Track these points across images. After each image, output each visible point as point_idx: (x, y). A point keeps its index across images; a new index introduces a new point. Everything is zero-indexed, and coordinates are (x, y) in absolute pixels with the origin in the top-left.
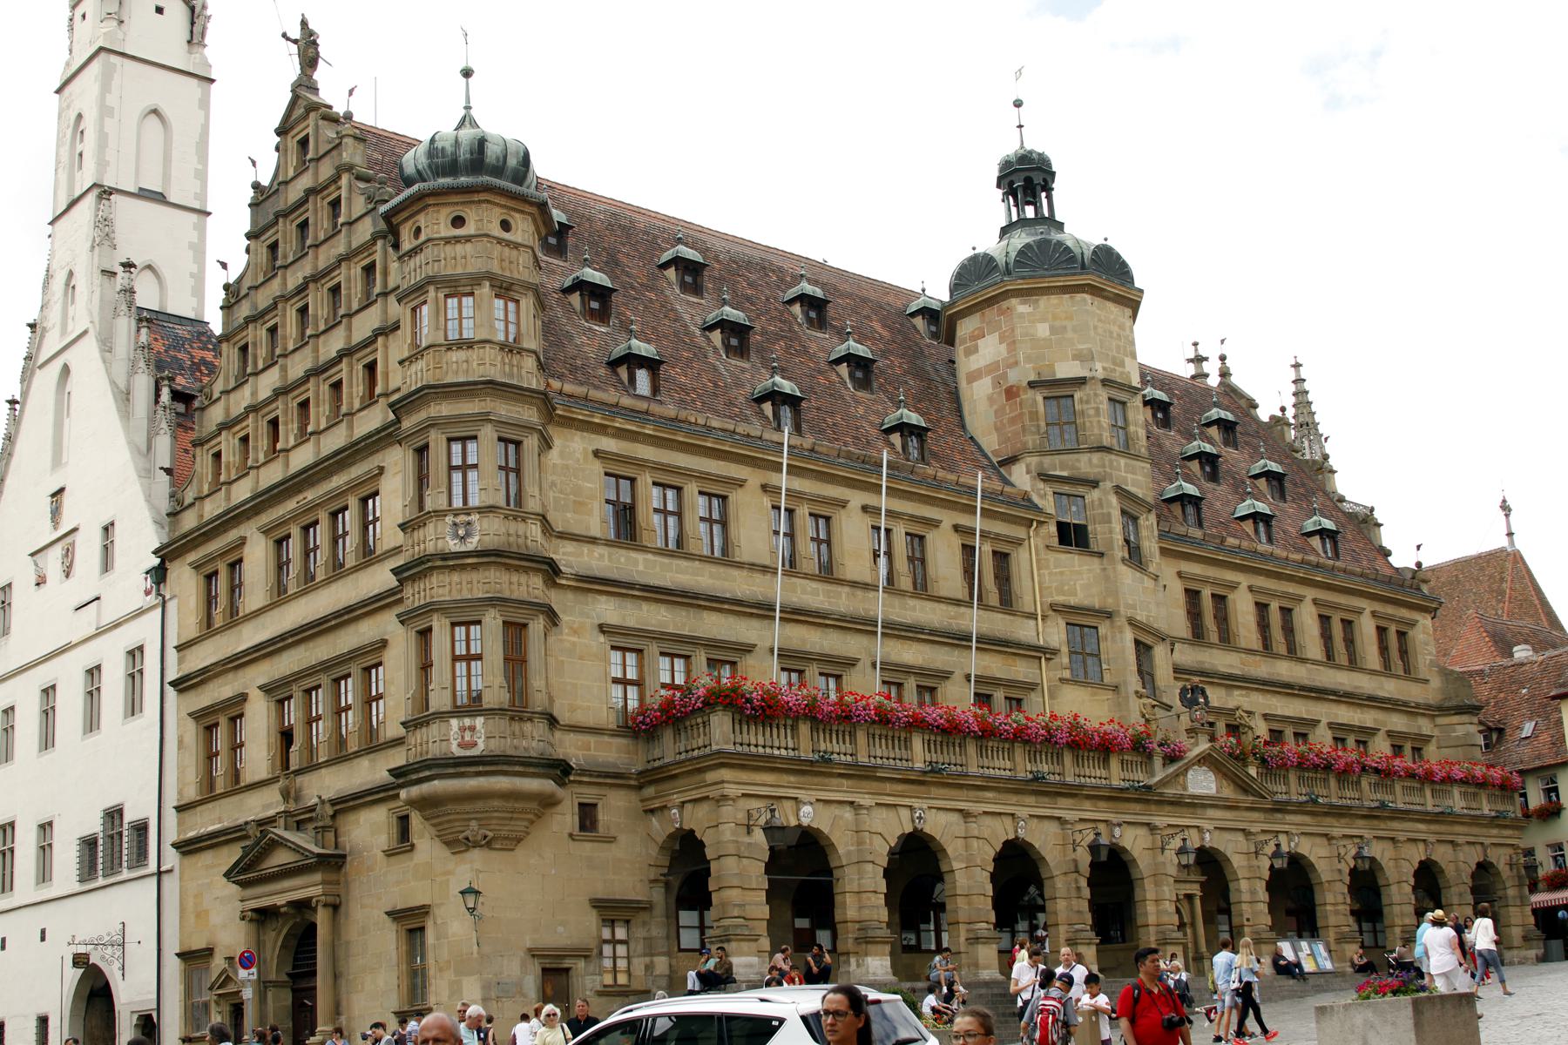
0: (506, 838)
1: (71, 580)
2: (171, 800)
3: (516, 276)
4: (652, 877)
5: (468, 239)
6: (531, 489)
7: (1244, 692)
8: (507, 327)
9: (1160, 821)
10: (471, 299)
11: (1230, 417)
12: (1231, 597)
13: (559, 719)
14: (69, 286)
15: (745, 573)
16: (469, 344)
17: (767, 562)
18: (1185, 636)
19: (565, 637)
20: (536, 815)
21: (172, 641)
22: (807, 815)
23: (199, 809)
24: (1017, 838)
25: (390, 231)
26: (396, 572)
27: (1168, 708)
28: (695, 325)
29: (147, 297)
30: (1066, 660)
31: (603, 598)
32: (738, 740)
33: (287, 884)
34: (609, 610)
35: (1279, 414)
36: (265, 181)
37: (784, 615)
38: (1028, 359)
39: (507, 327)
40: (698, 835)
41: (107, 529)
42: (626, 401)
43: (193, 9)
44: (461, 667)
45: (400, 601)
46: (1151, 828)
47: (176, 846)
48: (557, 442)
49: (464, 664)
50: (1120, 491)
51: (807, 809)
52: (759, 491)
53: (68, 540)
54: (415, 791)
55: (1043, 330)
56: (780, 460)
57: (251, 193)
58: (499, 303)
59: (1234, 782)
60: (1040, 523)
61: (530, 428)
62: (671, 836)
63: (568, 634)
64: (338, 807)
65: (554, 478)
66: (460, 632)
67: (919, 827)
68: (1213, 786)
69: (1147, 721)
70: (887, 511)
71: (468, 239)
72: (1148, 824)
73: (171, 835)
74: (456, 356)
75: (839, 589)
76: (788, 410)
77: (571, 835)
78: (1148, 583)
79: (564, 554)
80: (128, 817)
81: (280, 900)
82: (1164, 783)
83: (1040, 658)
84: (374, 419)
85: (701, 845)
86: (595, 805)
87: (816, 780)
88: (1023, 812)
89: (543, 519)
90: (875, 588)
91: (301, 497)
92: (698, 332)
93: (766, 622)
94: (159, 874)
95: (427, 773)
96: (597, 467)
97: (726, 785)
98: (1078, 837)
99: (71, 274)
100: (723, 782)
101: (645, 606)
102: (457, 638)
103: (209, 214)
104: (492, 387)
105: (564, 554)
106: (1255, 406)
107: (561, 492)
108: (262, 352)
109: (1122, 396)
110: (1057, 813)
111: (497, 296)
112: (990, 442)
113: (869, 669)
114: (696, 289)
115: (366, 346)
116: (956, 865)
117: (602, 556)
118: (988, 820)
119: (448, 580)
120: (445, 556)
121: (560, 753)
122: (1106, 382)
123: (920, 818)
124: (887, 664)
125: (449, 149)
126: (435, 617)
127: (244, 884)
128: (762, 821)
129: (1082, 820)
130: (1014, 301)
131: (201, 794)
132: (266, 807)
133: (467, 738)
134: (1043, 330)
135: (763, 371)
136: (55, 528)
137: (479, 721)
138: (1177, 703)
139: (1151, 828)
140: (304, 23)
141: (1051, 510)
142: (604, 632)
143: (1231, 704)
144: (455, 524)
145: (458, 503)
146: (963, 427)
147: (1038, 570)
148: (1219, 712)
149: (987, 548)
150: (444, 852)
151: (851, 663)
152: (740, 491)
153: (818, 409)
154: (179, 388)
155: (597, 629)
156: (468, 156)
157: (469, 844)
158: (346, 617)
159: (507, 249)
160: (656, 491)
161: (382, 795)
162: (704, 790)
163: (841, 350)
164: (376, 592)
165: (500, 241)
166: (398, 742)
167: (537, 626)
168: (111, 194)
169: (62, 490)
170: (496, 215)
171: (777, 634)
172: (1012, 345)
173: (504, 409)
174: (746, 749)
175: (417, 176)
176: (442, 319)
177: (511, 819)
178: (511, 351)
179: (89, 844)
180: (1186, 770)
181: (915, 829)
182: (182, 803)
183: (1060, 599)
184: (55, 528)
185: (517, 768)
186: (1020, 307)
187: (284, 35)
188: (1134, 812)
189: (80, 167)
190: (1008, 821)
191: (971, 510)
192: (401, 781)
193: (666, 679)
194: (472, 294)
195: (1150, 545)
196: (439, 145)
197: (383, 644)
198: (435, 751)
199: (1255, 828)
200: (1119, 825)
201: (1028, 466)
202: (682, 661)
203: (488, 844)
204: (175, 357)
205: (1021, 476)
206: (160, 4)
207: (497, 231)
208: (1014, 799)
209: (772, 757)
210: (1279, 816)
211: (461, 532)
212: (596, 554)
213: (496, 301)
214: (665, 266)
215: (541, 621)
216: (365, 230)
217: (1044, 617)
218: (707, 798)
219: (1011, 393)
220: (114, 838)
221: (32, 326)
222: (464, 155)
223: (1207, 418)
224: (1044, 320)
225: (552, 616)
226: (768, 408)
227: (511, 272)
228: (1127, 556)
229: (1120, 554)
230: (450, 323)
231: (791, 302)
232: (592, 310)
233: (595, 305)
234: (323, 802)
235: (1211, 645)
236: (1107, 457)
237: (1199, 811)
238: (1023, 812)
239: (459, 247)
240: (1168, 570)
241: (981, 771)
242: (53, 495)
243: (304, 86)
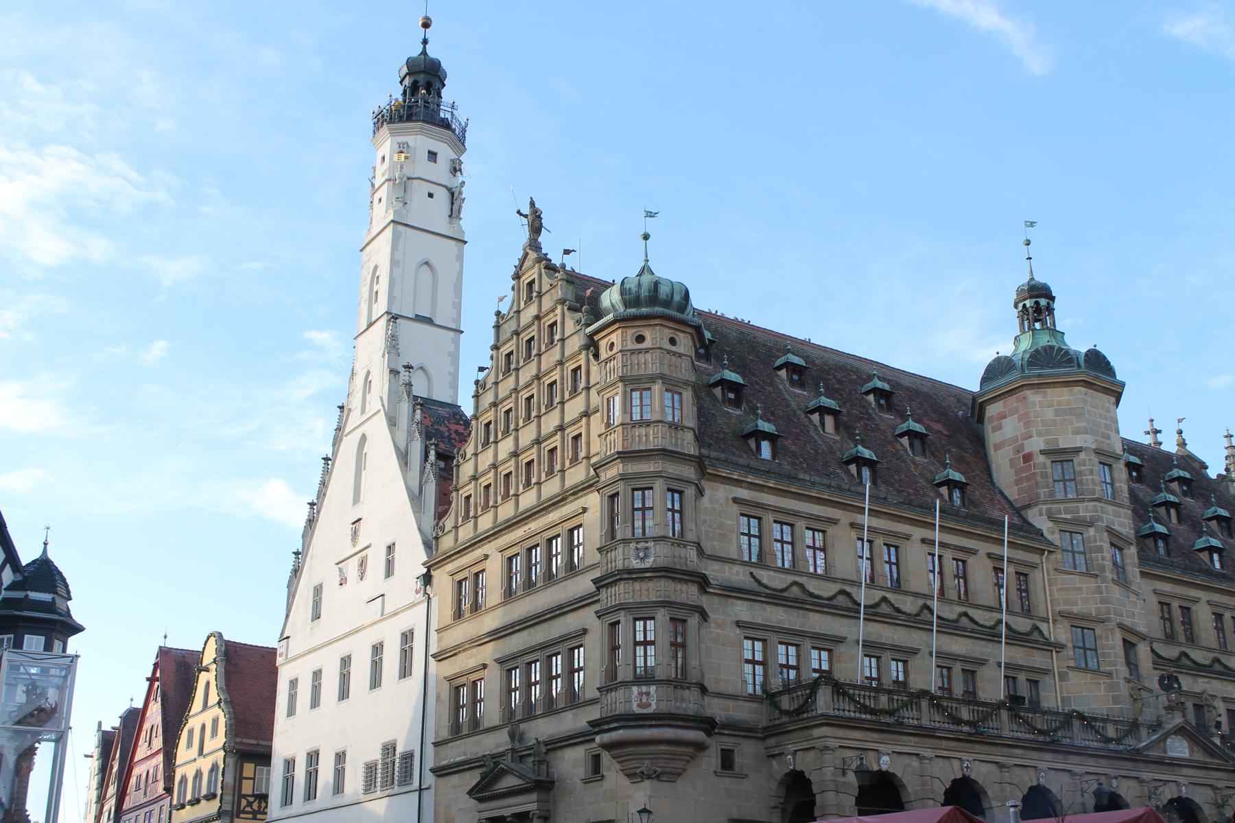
0: (671, 773)
1: (364, 582)
2: (430, 738)
3: (680, 376)
4: (772, 804)
5: (647, 351)
6: (690, 525)
7: (1206, 680)
8: (673, 412)
9: (1146, 776)
10: (649, 392)
11: (1188, 476)
12: (1194, 608)
13: (708, 688)
14: (367, 382)
16: (648, 424)
17: (854, 578)
18: (1160, 637)
19: (713, 630)
20: (691, 757)
21: (434, 626)
22: (885, 763)
23: (450, 745)
24: (1039, 785)
25: (592, 345)
26: (595, 581)
27: (1151, 691)
28: (801, 409)
29: (420, 390)
30: (1071, 653)
31: (739, 602)
32: (836, 706)
33: (512, 801)
34: (742, 610)
35: (1225, 473)
36: (504, 311)
37: (866, 617)
38: (1040, 434)
39: (673, 412)
40: (807, 775)
41: (390, 548)
42: (753, 463)
43: (453, 194)
44: (640, 651)
45: (598, 601)
46: (1140, 781)
47: (433, 770)
48: (707, 492)
49: (642, 648)
50: (1110, 531)
51: (885, 758)
52: (849, 527)
53: (363, 554)
54: (607, 737)
55: (1049, 414)
56: (863, 506)
57: (495, 318)
58: (668, 395)
59: (1202, 748)
60: (1050, 552)
61: (689, 482)
62: (786, 775)
63: (714, 628)
64: (550, 747)
65: (705, 517)
66: (639, 625)
67: (967, 774)
68: (1187, 751)
69: (1135, 700)
70: (939, 542)
72: (1137, 778)
73: (430, 763)
74: (637, 431)
75: (906, 598)
76: (867, 470)
77: (715, 772)
78: (1133, 598)
79: (712, 571)
80: (400, 750)
81: (507, 812)
82: (1147, 747)
83: (1052, 651)
84: (577, 475)
85: (809, 782)
86: (733, 751)
87: (892, 737)
88: (1043, 765)
89: (699, 547)
91: (526, 527)
92: (803, 416)
93: (854, 621)
94: (420, 790)
95: (615, 725)
96: (735, 509)
97: (828, 739)
98: (1085, 786)
99: (368, 372)
100: (826, 737)
101: (768, 608)
102: (638, 629)
104: (665, 453)
105: (712, 571)
106: (1206, 468)
107: (710, 527)
108: (501, 427)
109: (1108, 460)
110: (1068, 767)
111: (667, 390)
112: (1012, 493)
113: (927, 657)
114: (801, 384)
115: (574, 424)
116: (994, 804)
117: (738, 572)
118: (1017, 770)
119: (631, 588)
120: (630, 571)
121: (708, 712)
122: (1098, 452)
123: (967, 767)
124: (941, 653)
125: (634, 289)
126: (623, 613)
127: (481, 800)
128: (854, 766)
129: (1087, 773)
130: (1028, 393)
131: (452, 735)
132: (498, 746)
134: (1049, 414)
135: (849, 441)
136: (354, 546)
137: (653, 689)
138: (1156, 686)
139: (1140, 781)
140: (532, 204)
141: (1058, 543)
142: (739, 627)
143: (1198, 689)
144: (637, 549)
145: (639, 532)
146: (992, 482)
147: (1049, 586)
148: (1189, 694)
149: (1012, 570)
150: (626, 782)
151: (914, 652)
152: (834, 526)
153: (888, 469)
154: (441, 451)
155: (735, 625)
156: (647, 294)
157: (644, 776)
158: (558, 612)
159: (673, 358)
160: (777, 527)
161: (581, 739)
162: (811, 742)
163: (904, 427)
164: (579, 595)
165: (669, 352)
166: (593, 702)
167: (694, 621)
168: (396, 319)
169: (360, 520)
170: (668, 333)
171: (861, 629)
172: (1028, 424)
173: (673, 469)
174: (842, 713)
175: (611, 307)
176: (629, 406)
177: (674, 759)
178: (676, 428)
179: (370, 769)
180: (1166, 738)
181: (964, 775)
182: (438, 740)
184: (354, 546)
185: (679, 723)
186: (1033, 397)
187: (519, 212)
188: (1126, 768)
189: (376, 301)
191: (1000, 542)
192: (597, 730)
193: (782, 660)
194: (649, 389)
195: (1133, 571)
196: (627, 286)
197: (585, 632)
198: (620, 709)
199: (1221, 785)
200: (1116, 778)
202: (794, 648)
203: (657, 776)
204: (438, 429)
205: (1038, 518)
206: (431, 192)
207: (668, 346)
208: (1035, 755)
209: (861, 719)
211: (641, 555)
212: (734, 571)
213: (666, 393)
214: (780, 368)
215: (697, 618)
216: (575, 344)
217: (1054, 621)
218: (813, 748)
219: (1028, 458)
220: (388, 766)
221: (341, 408)
222: (644, 293)
223: (1170, 476)
225: (704, 615)
226: (853, 468)
227: (677, 373)
228: (1116, 578)
230: (634, 408)
231: (867, 393)
232: (730, 399)
233: (731, 396)
234: (539, 743)
237: (1177, 769)
238: (1043, 765)
239: (641, 356)
240: (1145, 587)
241: (1012, 734)
242: (353, 523)
243: (534, 245)
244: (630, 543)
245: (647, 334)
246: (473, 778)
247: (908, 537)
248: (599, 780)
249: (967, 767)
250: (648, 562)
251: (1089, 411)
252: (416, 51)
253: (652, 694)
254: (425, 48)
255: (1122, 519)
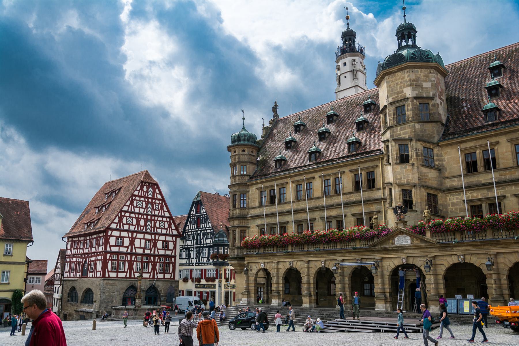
15: (287, 205)
22: (262, 266)
30: (388, 201)
60: (382, 159)
90: (323, 197)
110: (335, 258)
122: (391, 104)
190: (319, 263)
210: (449, 248)
229: (395, 162)
235: (481, 173)
236: (392, 129)
245: (236, 150)
247: (314, 178)
249: (291, 264)
251: (390, 86)
252: (345, 29)
254: (348, 26)
255: (407, 130)
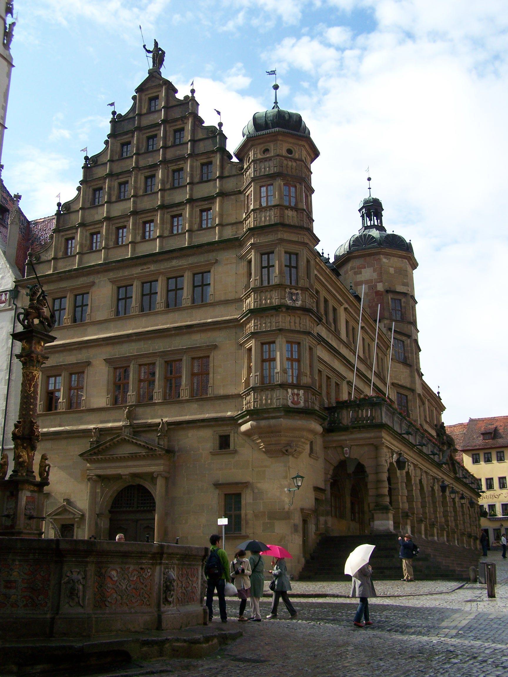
33: (130, 463)
55: (392, 270)
71: (295, 160)
103: (6, 128)
133: (296, 399)
137: (301, 392)
140: (156, 44)
172: (380, 275)
183: (396, 381)
201: (385, 324)
219: (378, 293)
224: (392, 267)
244: (286, 288)
246: (84, 445)
248: (232, 453)
250: (298, 304)
253: (301, 395)
